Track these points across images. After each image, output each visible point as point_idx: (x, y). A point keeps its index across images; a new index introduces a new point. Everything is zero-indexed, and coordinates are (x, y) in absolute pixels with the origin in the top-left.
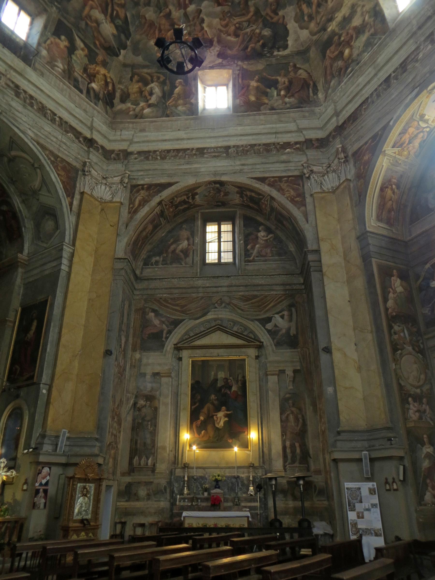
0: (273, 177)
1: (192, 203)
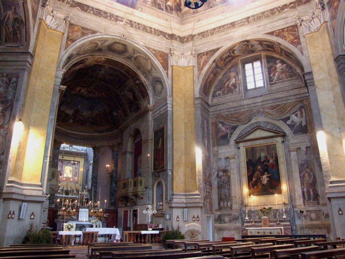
0: (278, 30)
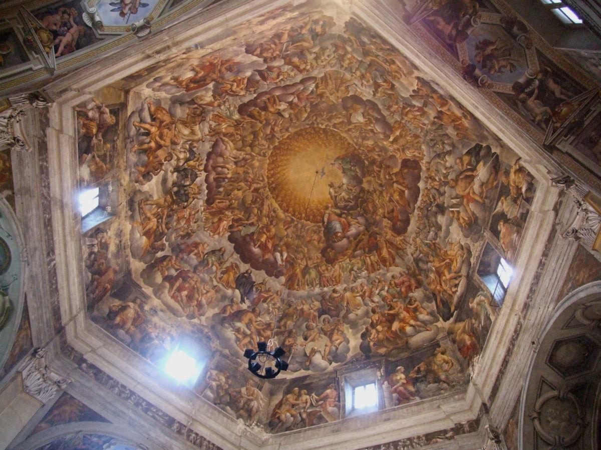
1: (540, 76)
